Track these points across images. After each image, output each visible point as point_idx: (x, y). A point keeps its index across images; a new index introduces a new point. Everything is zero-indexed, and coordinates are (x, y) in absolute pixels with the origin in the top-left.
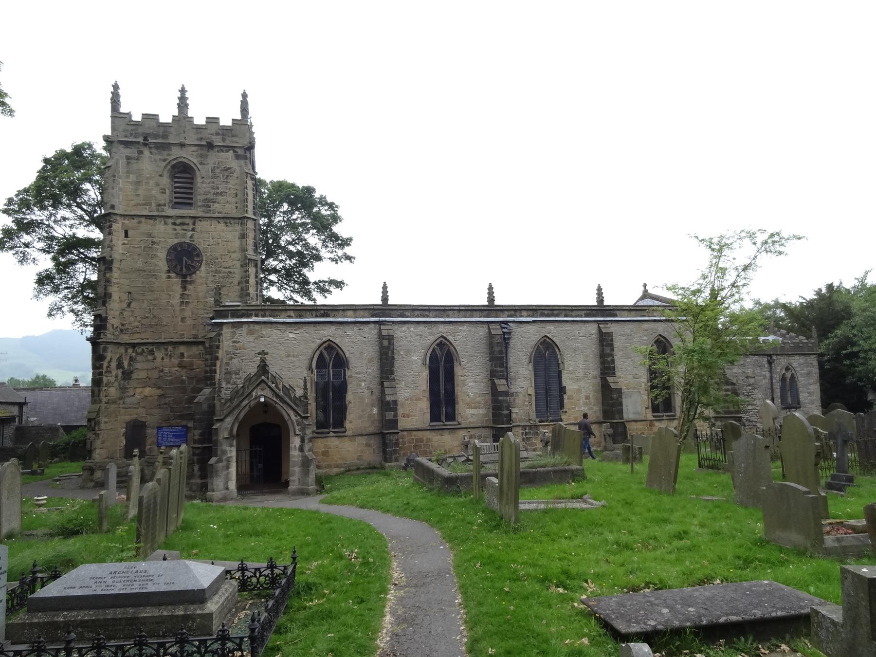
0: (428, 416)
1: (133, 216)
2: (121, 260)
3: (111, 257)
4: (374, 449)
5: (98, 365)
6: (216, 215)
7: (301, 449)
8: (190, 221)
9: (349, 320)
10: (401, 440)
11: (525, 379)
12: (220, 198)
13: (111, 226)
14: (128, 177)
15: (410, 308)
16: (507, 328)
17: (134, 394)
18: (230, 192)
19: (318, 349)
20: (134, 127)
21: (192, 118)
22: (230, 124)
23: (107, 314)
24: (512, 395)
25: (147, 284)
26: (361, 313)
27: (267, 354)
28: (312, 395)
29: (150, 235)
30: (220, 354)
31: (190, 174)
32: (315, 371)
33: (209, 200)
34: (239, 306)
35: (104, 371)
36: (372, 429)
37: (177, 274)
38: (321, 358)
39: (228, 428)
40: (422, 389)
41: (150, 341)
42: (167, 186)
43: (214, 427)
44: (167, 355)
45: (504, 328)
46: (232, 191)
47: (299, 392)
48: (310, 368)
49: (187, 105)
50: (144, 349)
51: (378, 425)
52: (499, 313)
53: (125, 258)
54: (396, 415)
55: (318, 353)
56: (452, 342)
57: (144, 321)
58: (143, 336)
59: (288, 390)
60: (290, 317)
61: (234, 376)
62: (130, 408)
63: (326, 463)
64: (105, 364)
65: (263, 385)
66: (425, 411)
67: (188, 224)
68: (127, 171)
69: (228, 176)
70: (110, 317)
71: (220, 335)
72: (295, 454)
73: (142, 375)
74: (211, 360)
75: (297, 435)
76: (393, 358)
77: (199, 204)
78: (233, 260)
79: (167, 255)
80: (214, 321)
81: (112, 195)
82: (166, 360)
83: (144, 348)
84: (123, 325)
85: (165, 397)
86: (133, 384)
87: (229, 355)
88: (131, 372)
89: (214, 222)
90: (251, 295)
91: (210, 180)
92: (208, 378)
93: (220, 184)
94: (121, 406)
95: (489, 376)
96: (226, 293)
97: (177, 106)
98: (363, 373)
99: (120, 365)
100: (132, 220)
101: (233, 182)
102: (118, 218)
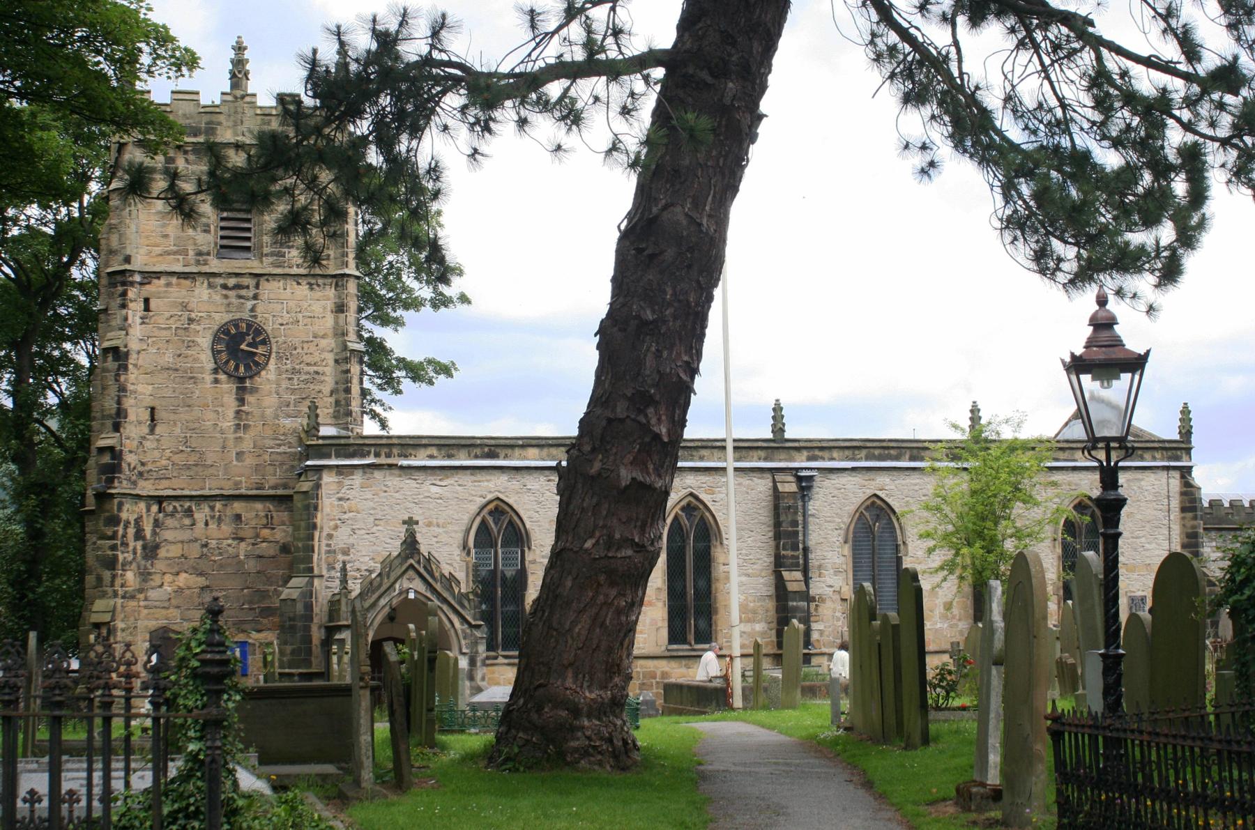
0: (664, 633)
2: (139, 352)
3: (126, 346)
11: (837, 572)
17: (163, 584)
19: (478, 514)
21: (254, 95)
24: (813, 599)
25: (181, 393)
27: (417, 523)
29: (185, 307)
30: (319, 519)
32: (473, 551)
37: (230, 376)
41: (186, 492)
44: (213, 517)
48: (465, 546)
49: (246, 75)
52: (794, 453)
55: (478, 520)
56: (709, 504)
57: (176, 458)
58: (176, 483)
59: (450, 580)
60: (431, 457)
62: (156, 607)
64: (121, 532)
66: (660, 624)
67: (248, 287)
70: (126, 450)
73: (173, 551)
78: (323, 350)
79: (213, 342)
82: (213, 526)
83: (177, 504)
84: (143, 464)
86: (160, 565)
88: (157, 547)
89: (291, 283)
95: (772, 567)
97: (229, 76)
99: (139, 535)
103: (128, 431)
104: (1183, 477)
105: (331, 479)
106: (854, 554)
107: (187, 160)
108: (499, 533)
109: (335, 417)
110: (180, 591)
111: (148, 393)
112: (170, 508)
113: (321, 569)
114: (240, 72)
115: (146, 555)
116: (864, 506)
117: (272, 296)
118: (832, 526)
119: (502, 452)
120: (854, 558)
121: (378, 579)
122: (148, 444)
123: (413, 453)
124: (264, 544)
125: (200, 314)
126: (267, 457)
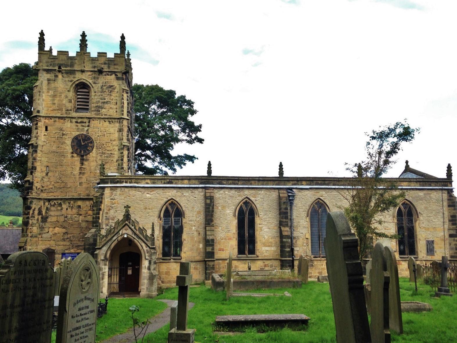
0: (236, 250)
1: (51, 118)
2: (43, 146)
3: (36, 143)
4: (199, 272)
5: (27, 213)
6: (104, 116)
7: (149, 269)
8: (87, 120)
9: (185, 186)
10: (218, 266)
11: (304, 227)
12: (106, 105)
13: (37, 124)
14: (48, 92)
15: (226, 178)
16: (291, 193)
17: (49, 232)
18: (112, 101)
19: (165, 204)
20: (52, 60)
21: (90, 53)
22: (113, 57)
23: (33, 180)
24: (295, 238)
25: (59, 161)
26: (194, 181)
27: (130, 207)
28: (158, 234)
29: (61, 129)
30: (102, 207)
31: (87, 89)
32: (163, 219)
33: (99, 107)
34: (115, 176)
35: (30, 216)
36: (198, 258)
37: (78, 155)
38: (167, 210)
39: (103, 254)
40: (232, 233)
41: (59, 197)
42: (73, 98)
43: (95, 253)
45: (289, 193)
46: (114, 101)
47: (149, 233)
48: (159, 217)
50: (56, 202)
51: (202, 255)
52: (286, 182)
53: (45, 144)
54: (213, 249)
55: (165, 207)
56: (254, 201)
57: (56, 185)
58: (55, 194)
59: (142, 230)
60: (147, 183)
61: (111, 221)
62: (45, 240)
63: (168, 280)
64: (31, 212)
65: (126, 227)
66: (234, 247)
67: (86, 122)
68: (48, 88)
69: (111, 91)
70: (35, 182)
71: (102, 194)
72: (145, 272)
73: (54, 219)
74: (97, 210)
75: (147, 259)
76: (213, 211)
77: (93, 109)
78: (114, 146)
79: (72, 142)
80: (99, 185)
81: (39, 104)
82: (69, 210)
83: (55, 202)
84: (43, 187)
85: (68, 234)
86: (47, 225)
87: (108, 208)
88: (47, 218)
89: (102, 121)
90: (124, 169)
91: (100, 94)
92: (95, 223)
93: (107, 96)
94: (40, 239)
95: (278, 225)
96: (109, 167)
97: (79, 46)
98: (194, 221)
99: (40, 213)
100: (50, 120)
101: (114, 94)
102: (42, 118)
103: (36, 174)
104: (448, 193)
105: (108, 192)
106: (311, 221)
107: (63, 76)
108: (173, 212)
109: (117, 170)
110: (55, 234)
111: (46, 161)
112: (53, 203)
113: (102, 226)
114: (83, 44)
115: (43, 221)
116: (315, 203)
117: (95, 126)
118: (302, 210)
119: (174, 182)
120: (311, 223)
121: (113, 229)
122: (45, 180)
123: (140, 182)
124: (89, 217)
125: (67, 132)
126: (91, 184)
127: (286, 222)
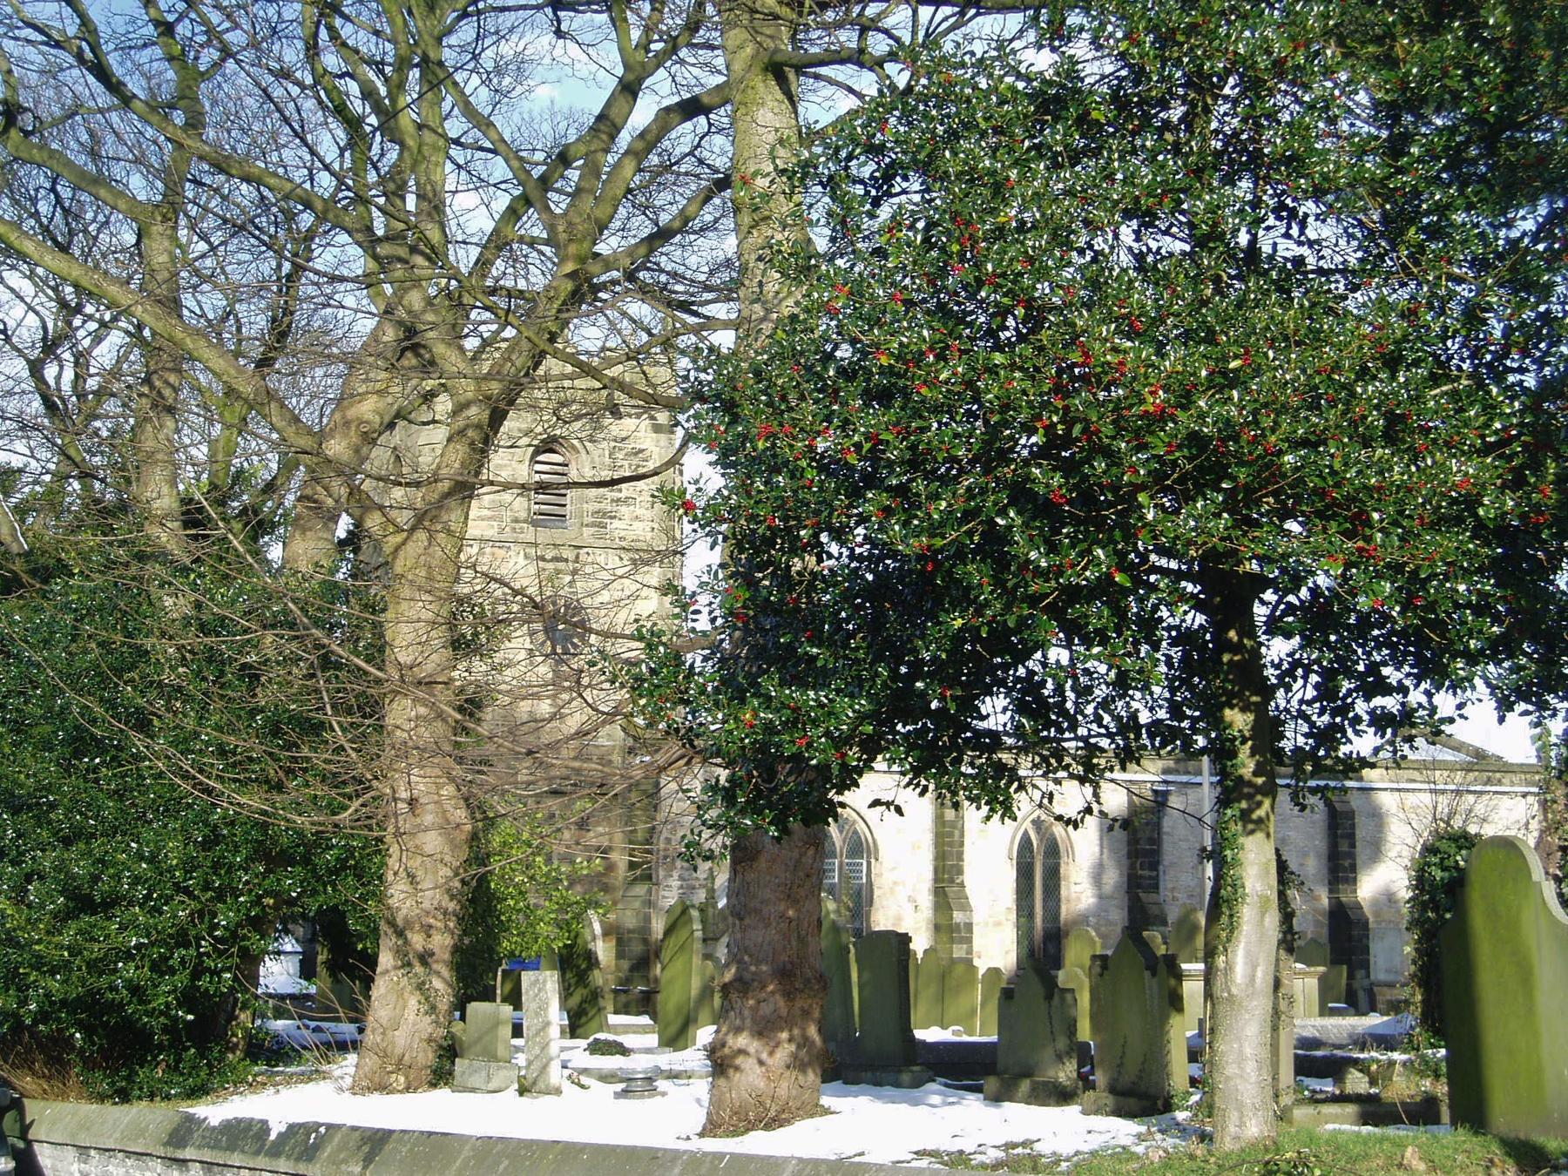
12: (623, 509)
54: (970, 951)
127: (1150, 878)
